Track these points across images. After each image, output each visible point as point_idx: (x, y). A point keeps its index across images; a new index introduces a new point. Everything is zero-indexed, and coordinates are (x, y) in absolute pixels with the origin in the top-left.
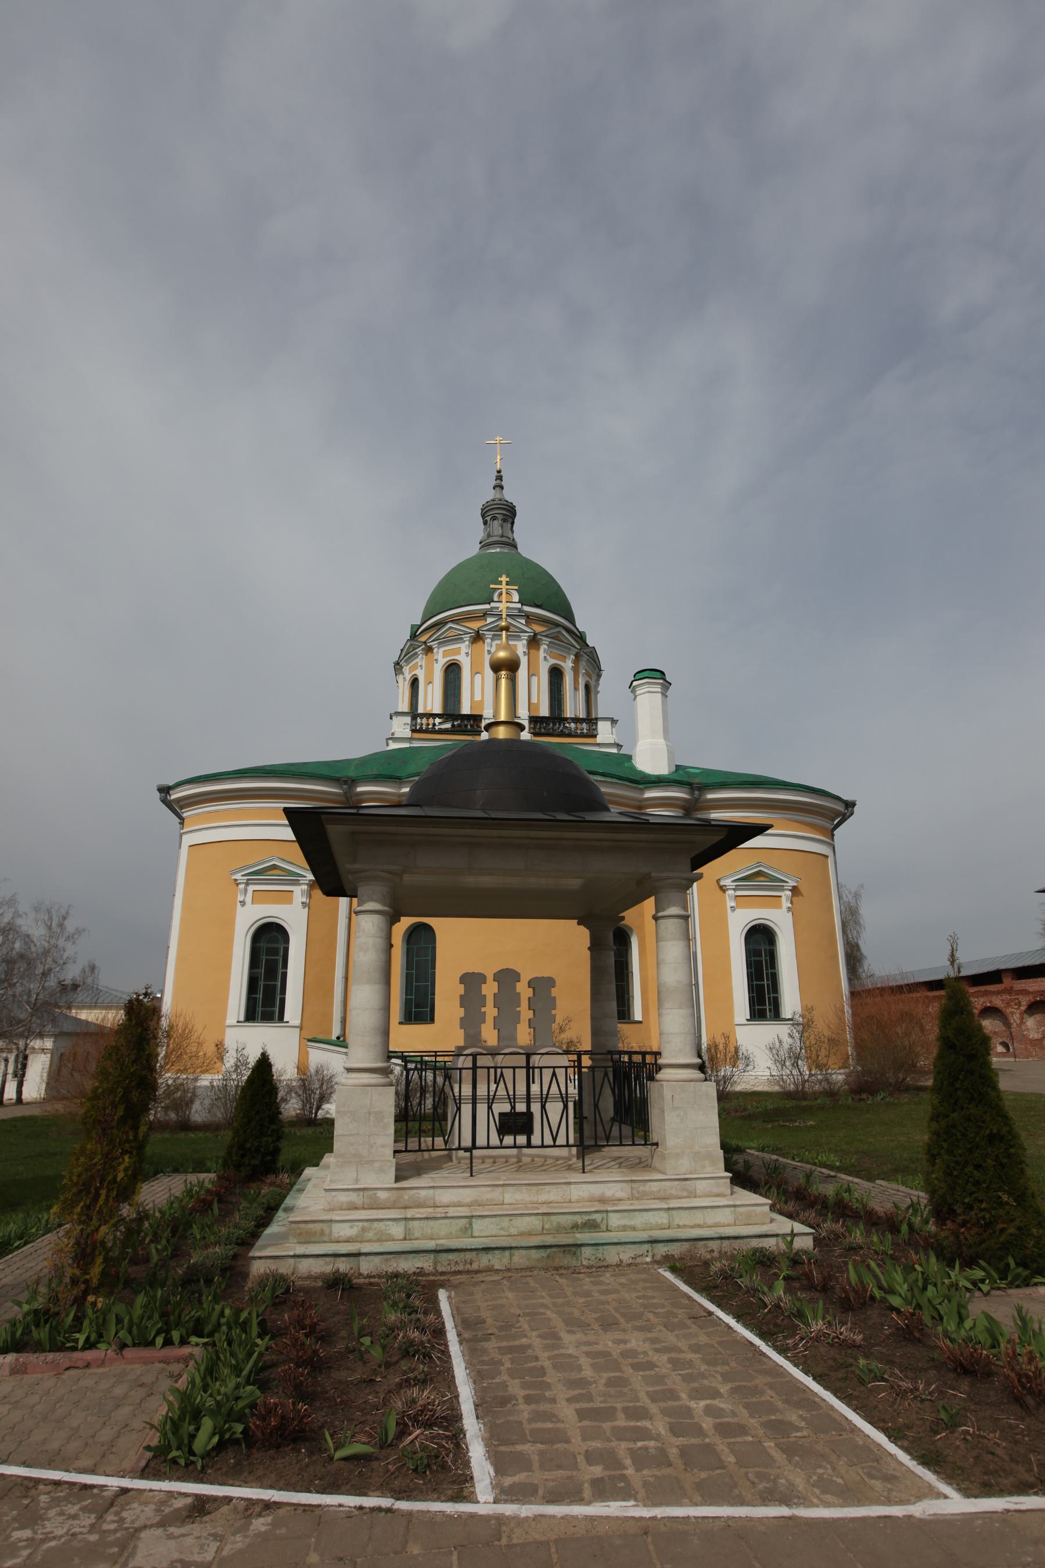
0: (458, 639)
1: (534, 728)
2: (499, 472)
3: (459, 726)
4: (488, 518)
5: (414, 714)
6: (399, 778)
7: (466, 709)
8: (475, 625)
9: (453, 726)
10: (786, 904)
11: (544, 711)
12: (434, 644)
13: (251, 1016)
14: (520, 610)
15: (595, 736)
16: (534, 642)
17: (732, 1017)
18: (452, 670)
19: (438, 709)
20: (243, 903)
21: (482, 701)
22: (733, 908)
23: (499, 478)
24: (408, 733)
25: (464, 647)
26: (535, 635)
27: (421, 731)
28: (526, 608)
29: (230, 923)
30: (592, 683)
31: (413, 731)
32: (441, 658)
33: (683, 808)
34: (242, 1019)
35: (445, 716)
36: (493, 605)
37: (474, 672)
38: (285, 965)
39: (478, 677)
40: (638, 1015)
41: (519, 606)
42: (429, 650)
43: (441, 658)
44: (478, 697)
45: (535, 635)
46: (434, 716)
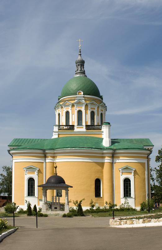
0: (68, 106)
1: (87, 128)
2: (80, 50)
3: (69, 128)
4: (77, 65)
5: (59, 126)
6: (54, 149)
7: (71, 124)
8: (73, 102)
9: (68, 128)
10: (133, 174)
11: (89, 124)
12: (63, 106)
13: (29, 195)
14: (84, 97)
15: (101, 129)
16: (86, 105)
17: (120, 196)
18: (67, 113)
19: (64, 124)
20: (26, 174)
21: (74, 121)
22: (121, 175)
23: (80, 52)
24: (57, 130)
25: (70, 108)
26: (87, 104)
27: (60, 129)
28: (85, 96)
29: (24, 178)
30: (103, 113)
31: (59, 129)
32: (65, 110)
33: (112, 154)
34: (27, 195)
35: (66, 126)
36: (77, 96)
37: (72, 114)
38: (34, 186)
39: (73, 115)
40: (101, 196)
41: (83, 96)
42: (62, 107)
43: (65, 110)
44: (73, 120)
45: (87, 104)
46: (63, 126)
